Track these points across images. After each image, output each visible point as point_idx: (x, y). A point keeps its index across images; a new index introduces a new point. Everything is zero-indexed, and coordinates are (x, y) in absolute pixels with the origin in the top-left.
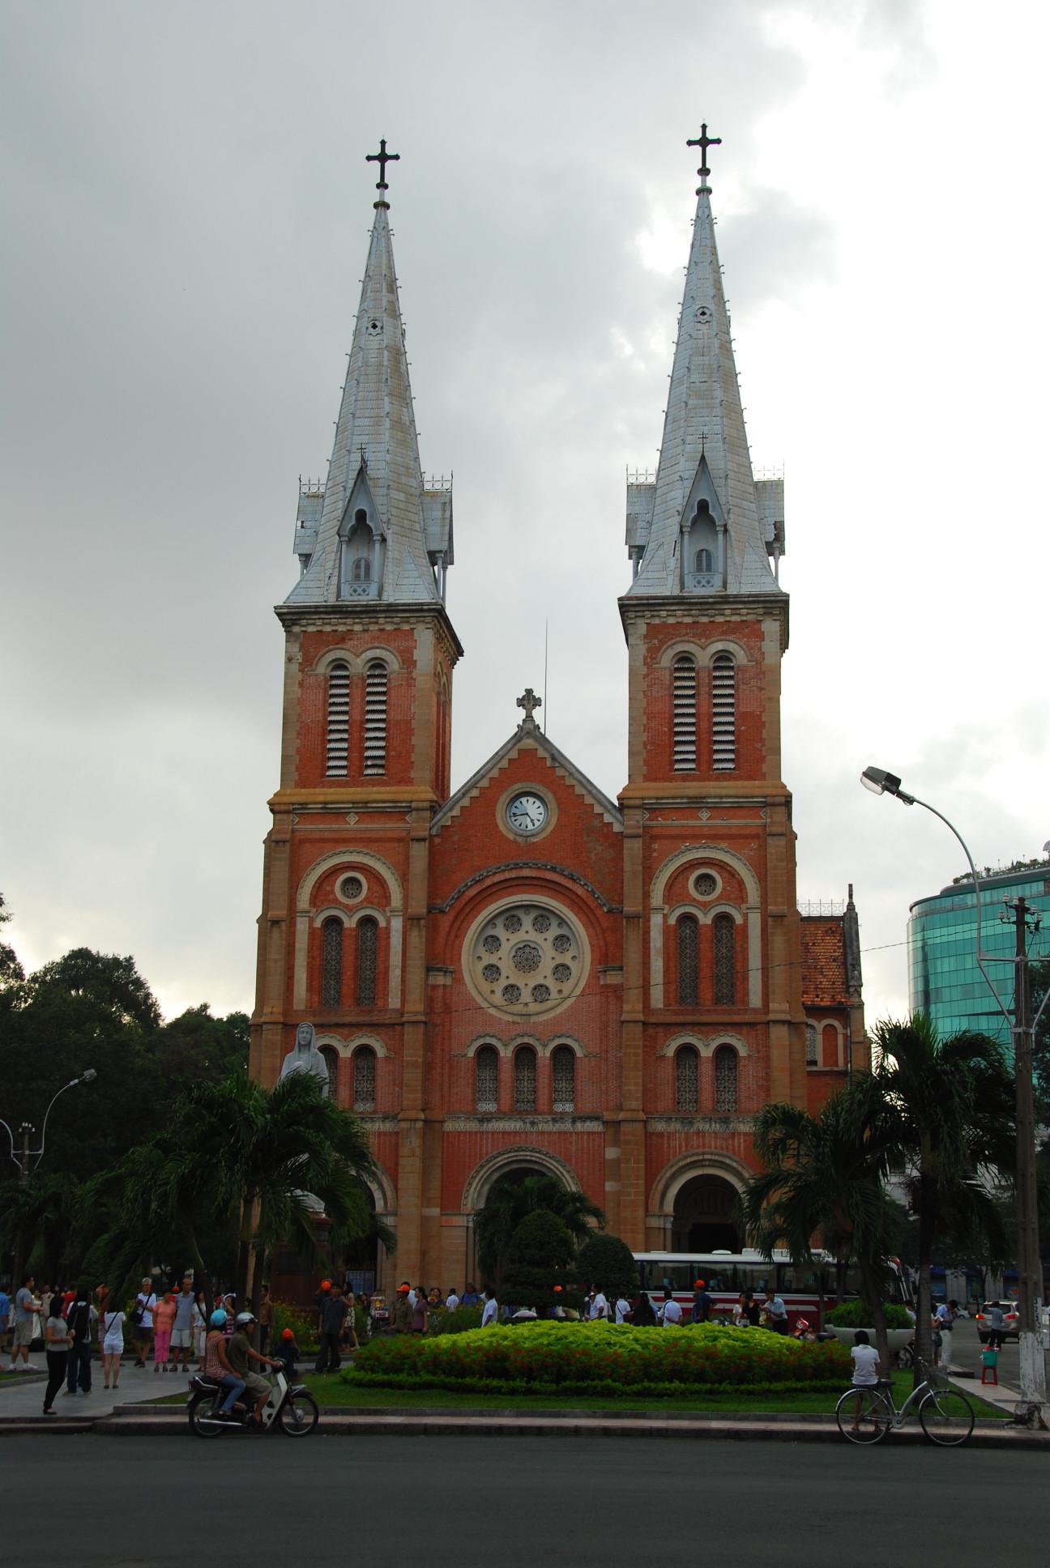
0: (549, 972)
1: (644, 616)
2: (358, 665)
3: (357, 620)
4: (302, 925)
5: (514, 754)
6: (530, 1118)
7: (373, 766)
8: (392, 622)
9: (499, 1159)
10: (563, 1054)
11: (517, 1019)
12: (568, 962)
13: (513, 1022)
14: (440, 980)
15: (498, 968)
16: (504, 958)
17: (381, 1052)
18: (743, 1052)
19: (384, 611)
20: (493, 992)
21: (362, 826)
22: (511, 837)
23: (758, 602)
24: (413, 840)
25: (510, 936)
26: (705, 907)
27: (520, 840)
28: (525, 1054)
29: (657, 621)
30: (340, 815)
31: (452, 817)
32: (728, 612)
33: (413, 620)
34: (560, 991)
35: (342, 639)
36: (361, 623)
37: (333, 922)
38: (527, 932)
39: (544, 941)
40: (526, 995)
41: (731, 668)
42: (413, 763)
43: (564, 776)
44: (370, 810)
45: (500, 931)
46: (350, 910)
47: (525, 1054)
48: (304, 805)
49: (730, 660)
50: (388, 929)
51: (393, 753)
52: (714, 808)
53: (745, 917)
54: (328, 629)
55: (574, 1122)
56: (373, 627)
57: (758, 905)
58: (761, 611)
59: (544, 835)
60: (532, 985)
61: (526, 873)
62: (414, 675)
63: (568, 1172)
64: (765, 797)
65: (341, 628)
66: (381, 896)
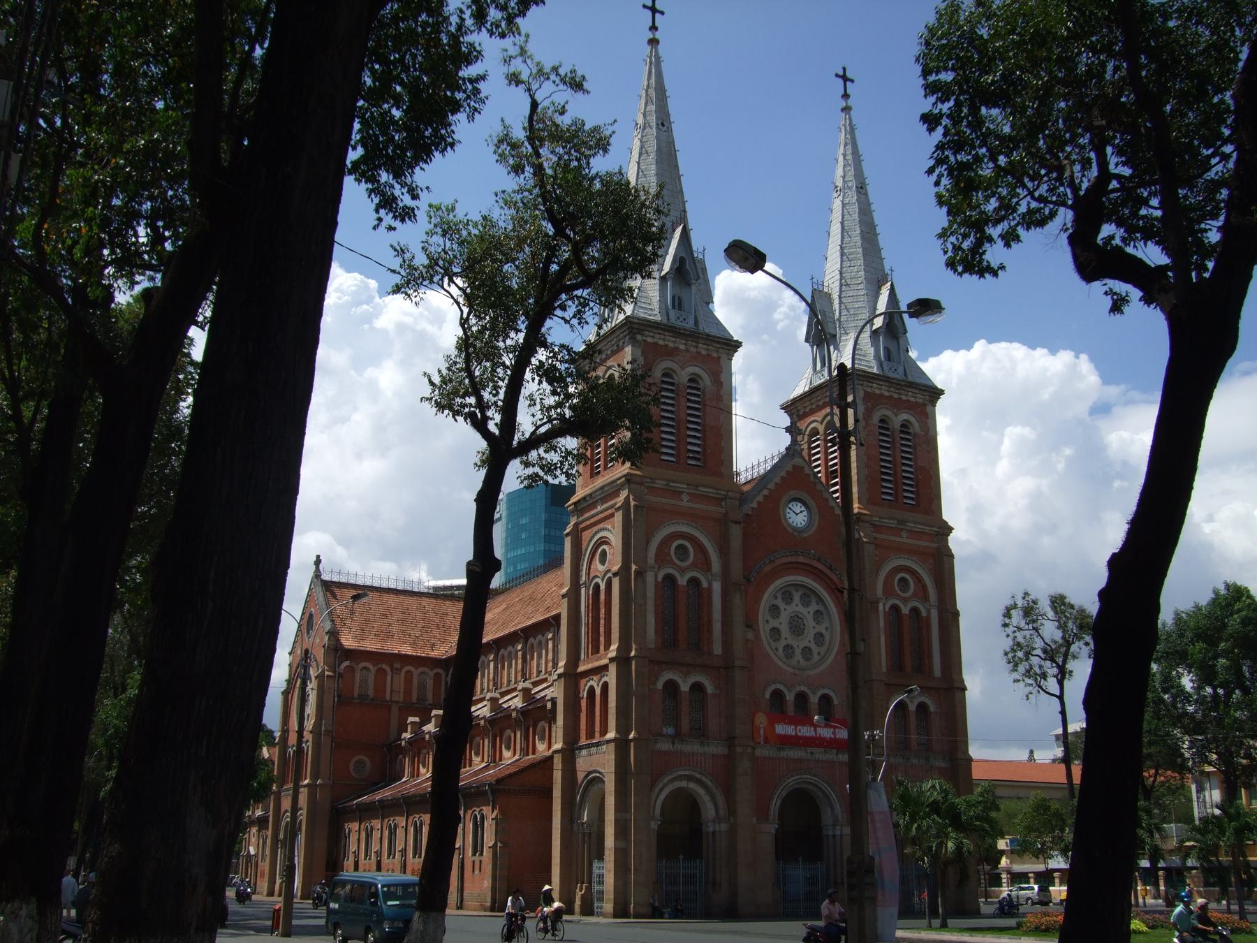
0: (811, 637)
1: (862, 385)
2: (683, 376)
3: (683, 341)
4: (650, 577)
5: (790, 469)
6: (809, 750)
7: (693, 458)
8: (707, 349)
9: (791, 780)
10: (825, 699)
11: (796, 671)
12: (824, 632)
13: (795, 674)
14: (750, 635)
15: (778, 631)
16: (783, 623)
17: (710, 689)
18: (932, 709)
19: (703, 338)
20: (777, 649)
21: (693, 505)
22: (790, 530)
23: (929, 391)
24: (732, 522)
25: (787, 607)
26: (905, 600)
27: (795, 533)
28: (802, 698)
29: (869, 390)
30: (677, 494)
31: (753, 508)
32: (910, 393)
33: (721, 350)
34: (819, 653)
35: (671, 353)
36: (685, 344)
37: (670, 579)
38: (796, 606)
39: (808, 612)
40: (798, 652)
41: (909, 433)
42: (722, 461)
43: (821, 491)
44: (697, 492)
45: (779, 602)
46: (683, 571)
47: (802, 698)
48: (653, 480)
49: (909, 428)
50: (710, 590)
51: (709, 451)
52: (912, 533)
53: (928, 611)
54: (661, 342)
55: (837, 754)
56: (693, 350)
57: (936, 604)
58: (927, 398)
59: (811, 533)
60: (801, 647)
61: (801, 559)
62: (722, 393)
63: (834, 792)
64: (939, 528)
65: (671, 345)
66: (704, 563)
